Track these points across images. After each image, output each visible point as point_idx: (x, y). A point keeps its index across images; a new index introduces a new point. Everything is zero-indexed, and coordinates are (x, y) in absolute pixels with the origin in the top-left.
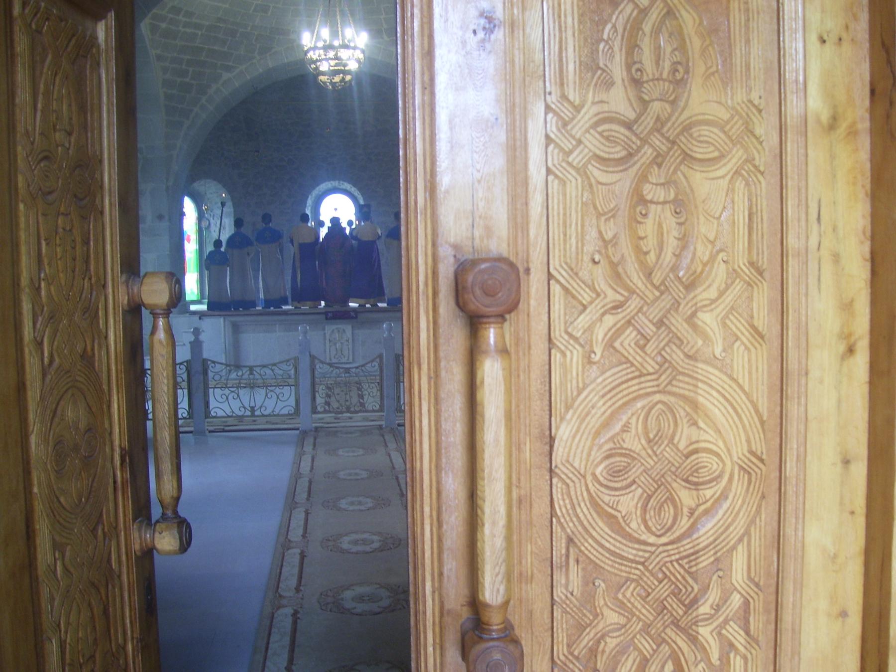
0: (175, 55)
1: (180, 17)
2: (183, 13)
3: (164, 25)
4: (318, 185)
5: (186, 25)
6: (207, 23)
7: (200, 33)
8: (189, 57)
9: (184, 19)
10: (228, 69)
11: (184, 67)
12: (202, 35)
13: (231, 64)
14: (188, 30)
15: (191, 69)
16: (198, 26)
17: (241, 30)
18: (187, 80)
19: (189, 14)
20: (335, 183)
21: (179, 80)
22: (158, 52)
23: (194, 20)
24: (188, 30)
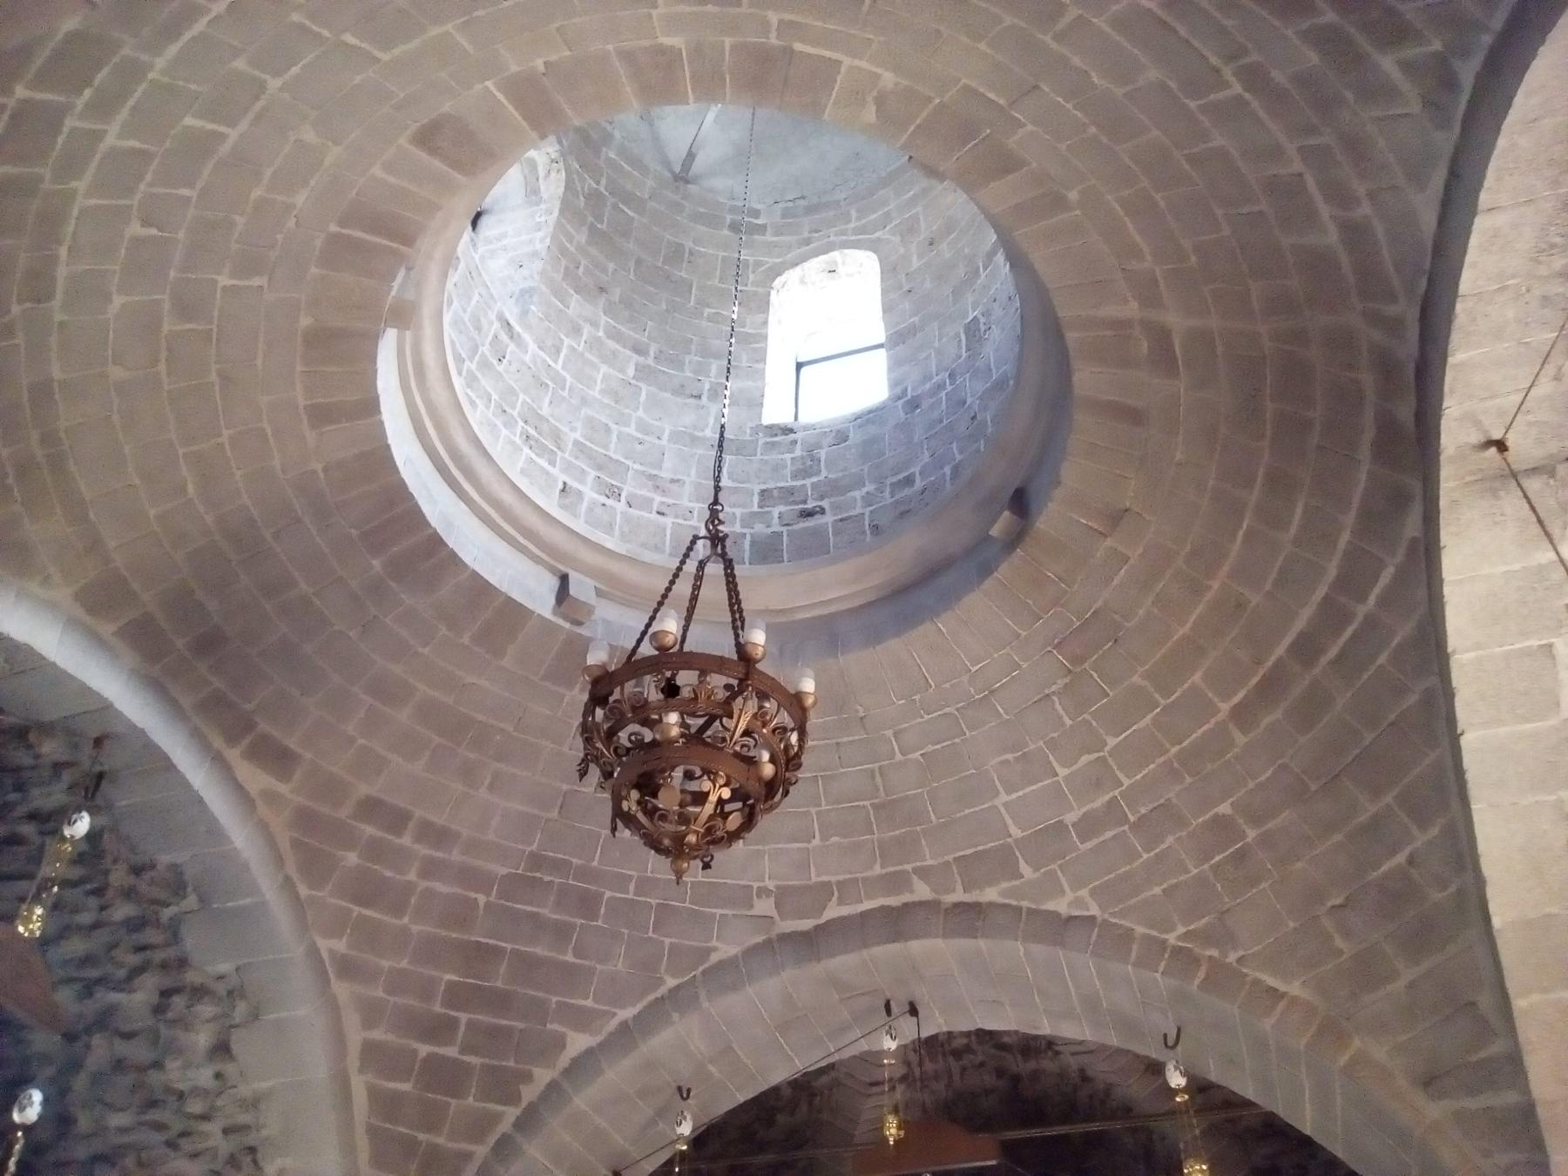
0: (404, 964)
1: (406, 840)
2: (411, 825)
3: (352, 858)
5: (430, 869)
6: (504, 871)
7: (482, 899)
8: (455, 978)
9: (424, 850)
10: (582, 1018)
11: (438, 1008)
12: (488, 905)
13: (589, 1003)
14: (441, 887)
15: (463, 1017)
16: (469, 877)
17: (608, 894)
18: (451, 1052)
19: (438, 836)
21: (424, 1049)
22: (341, 945)
23: (456, 856)
24: (441, 887)
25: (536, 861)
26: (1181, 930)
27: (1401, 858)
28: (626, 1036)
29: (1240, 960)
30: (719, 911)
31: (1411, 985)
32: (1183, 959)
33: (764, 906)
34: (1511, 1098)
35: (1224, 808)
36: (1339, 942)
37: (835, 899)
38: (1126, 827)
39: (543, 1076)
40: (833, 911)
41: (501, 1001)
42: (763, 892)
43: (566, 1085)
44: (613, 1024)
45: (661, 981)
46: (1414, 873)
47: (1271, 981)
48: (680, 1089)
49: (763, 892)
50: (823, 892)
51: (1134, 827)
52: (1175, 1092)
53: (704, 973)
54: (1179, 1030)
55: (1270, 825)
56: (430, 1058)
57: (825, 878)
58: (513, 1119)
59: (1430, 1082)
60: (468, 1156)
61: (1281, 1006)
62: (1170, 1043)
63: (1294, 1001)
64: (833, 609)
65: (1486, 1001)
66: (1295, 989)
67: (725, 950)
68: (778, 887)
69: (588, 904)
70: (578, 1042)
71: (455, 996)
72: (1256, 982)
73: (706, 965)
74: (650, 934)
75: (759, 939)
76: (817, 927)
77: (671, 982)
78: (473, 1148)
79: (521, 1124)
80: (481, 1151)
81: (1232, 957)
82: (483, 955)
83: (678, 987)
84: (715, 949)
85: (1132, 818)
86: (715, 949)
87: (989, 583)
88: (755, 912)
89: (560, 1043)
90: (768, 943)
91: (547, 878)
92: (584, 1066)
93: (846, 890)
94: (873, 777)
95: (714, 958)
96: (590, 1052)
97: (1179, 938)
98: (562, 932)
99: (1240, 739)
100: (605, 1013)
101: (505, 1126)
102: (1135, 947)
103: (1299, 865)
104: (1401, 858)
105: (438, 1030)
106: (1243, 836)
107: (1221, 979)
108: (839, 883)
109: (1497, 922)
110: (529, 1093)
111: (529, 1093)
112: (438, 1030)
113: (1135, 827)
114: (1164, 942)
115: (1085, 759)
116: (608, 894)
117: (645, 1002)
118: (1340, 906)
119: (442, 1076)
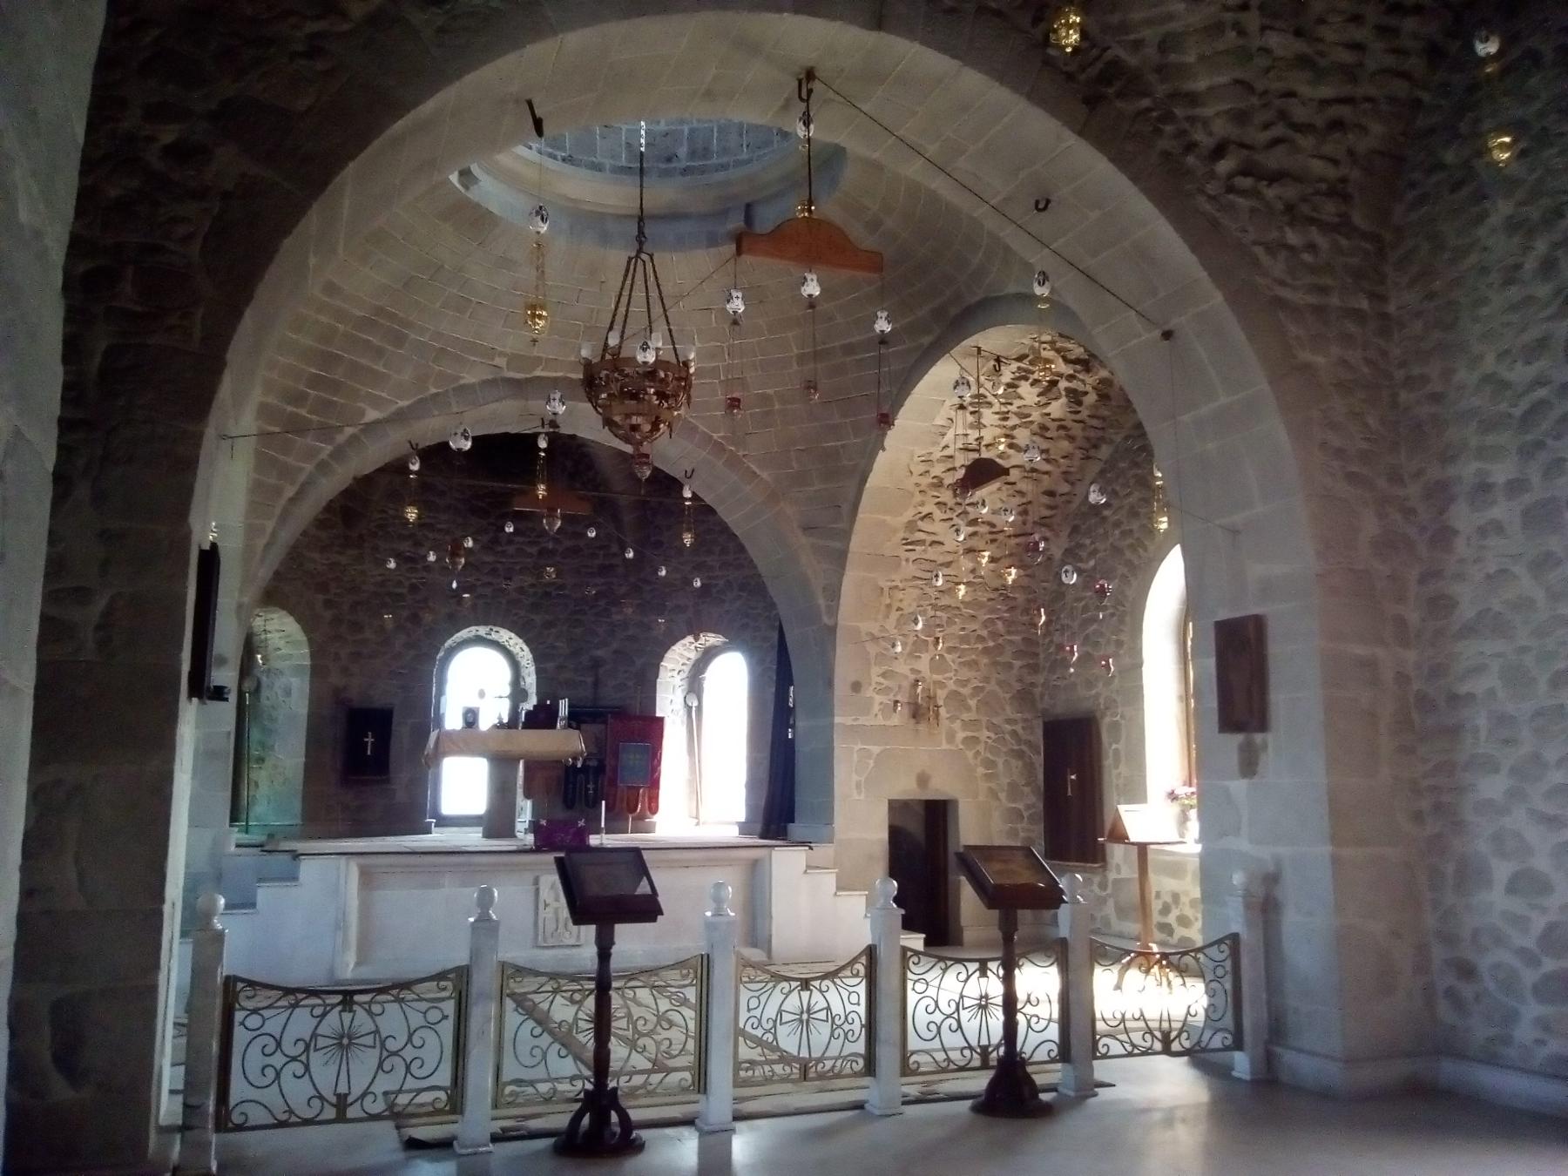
4: (458, 631)
10: (377, 403)
11: (302, 387)
13: (383, 395)
14: (323, 319)
18: (303, 412)
20: (482, 630)
21: (290, 409)
25: (380, 311)
26: (722, 434)
27: (839, 443)
28: (400, 417)
29: (744, 456)
30: (473, 358)
31: (815, 491)
32: (719, 448)
33: (501, 361)
34: (837, 545)
35: (770, 391)
36: (794, 464)
37: (541, 367)
38: (717, 381)
39: (349, 431)
40: (538, 373)
41: (335, 386)
42: (501, 354)
43: (363, 438)
44: (393, 408)
45: (428, 389)
46: (841, 451)
47: (754, 467)
48: (410, 442)
49: (501, 354)
50: (537, 361)
51: (721, 382)
52: (687, 499)
53: (454, 389)
54: (693, 471)
55: (789, 407)
56: (291, 413)
57: (541, 355)
58: (328, 452)
59: (808, 529)
60: (301, 469)
61: (756, 481)
62: (688, 475)
63: (762, 479)
64: (604, 210)
65: (846, 508)
66: (765, 475)
67: (469, 378)
68: (512, 354)
69: (399, 339)
70: (372, 415)
71: (315, 382)
72: (748, 467)
73: (456, 385)
74: (431, 364)
75: (490, 377)
76: (526, 379)
77: (433, 390)
78: (304, 465)
79: (331, 455)
80: (309, 467)
81: (741, 453)
82: (329, 360)
83: (437, 394)
84: (463, 378)
85: (722, 378)
86: (463, 378)
87: (713, 250)
88: (495, 363)
89: (363, 414)
90: (493, 383)
91: (382, 321)
92: (371, 427)
93: (549, 363)
94: (592, 312)
95: (462, 382)
96: (377, 422)
97: (719, 437)
98: (379, 353)
99: (795, 367)
100: (391, 401)
101: (324, 455)
102: (698, 436)
103: (793, 427)
104: (839, 443)
105: (299, 399)
106: (774, 406)
107: (734, 462)
108: (547, 360)
109: (867, 485)
110: (341, 438)
111: (341, 438)
112: (299, 399)
113: (721, 382)
114: (712, 436)
115: (712, 343)
116: (413, 336)
117: (415, 399)
118: (802, 450)
119: (297, 427)
